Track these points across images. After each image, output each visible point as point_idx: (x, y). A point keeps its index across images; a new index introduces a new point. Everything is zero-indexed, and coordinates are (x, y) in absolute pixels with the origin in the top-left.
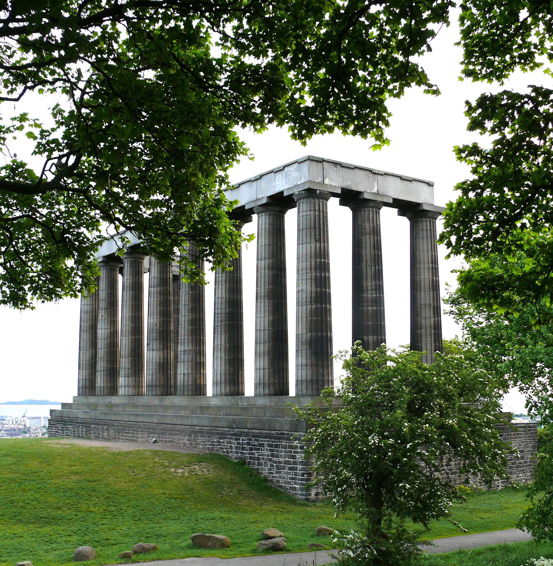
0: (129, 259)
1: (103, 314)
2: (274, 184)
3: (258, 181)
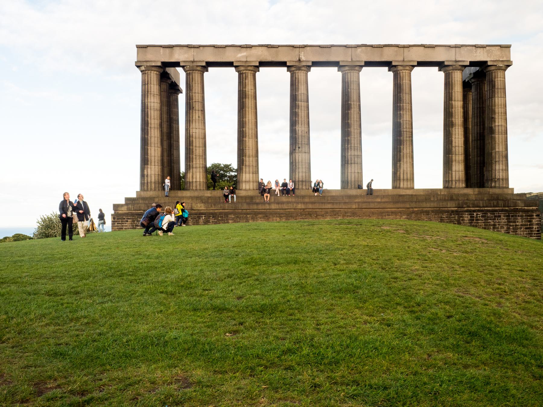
0: (252, 72)
1: (200, 115)
2: (475, 55)
3: (457, 49)
